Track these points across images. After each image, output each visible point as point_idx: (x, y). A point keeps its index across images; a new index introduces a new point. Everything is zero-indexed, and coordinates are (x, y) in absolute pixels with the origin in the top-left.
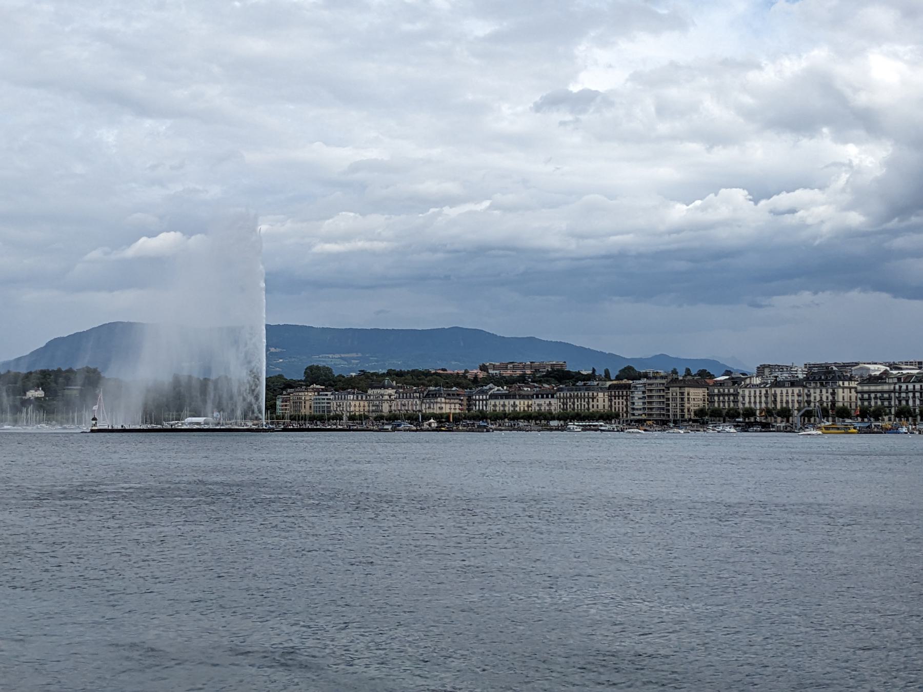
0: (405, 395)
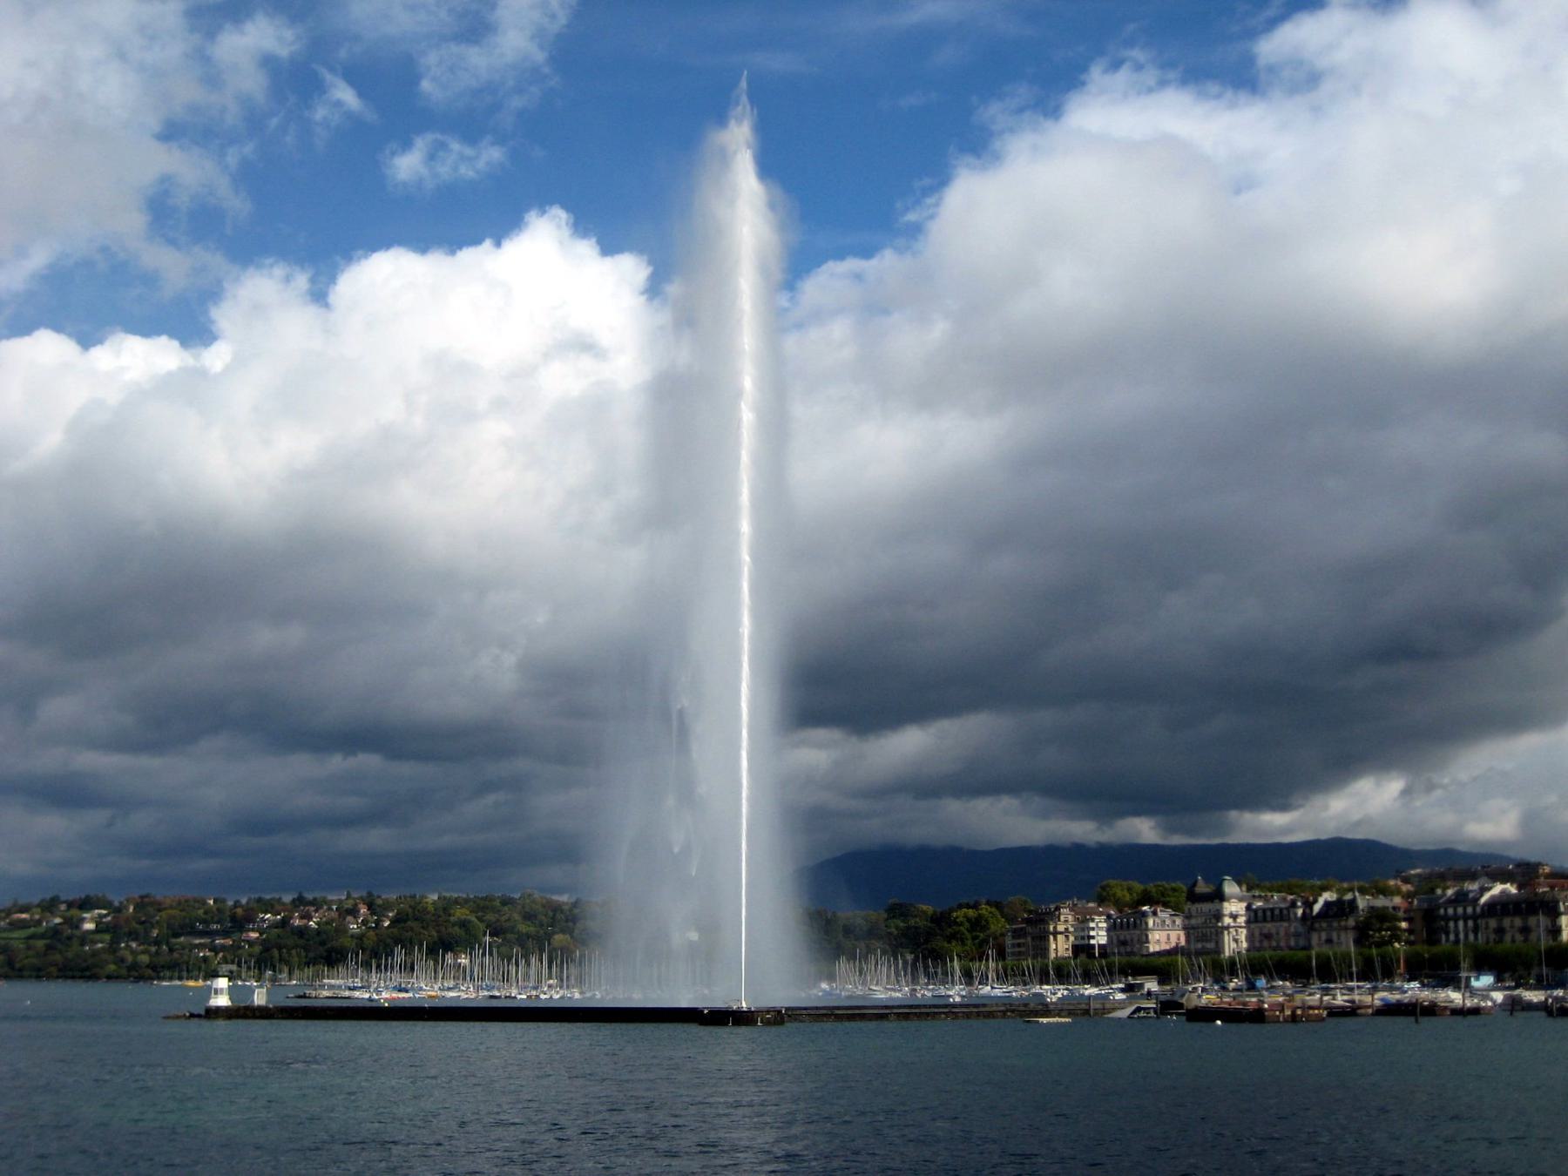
0: (1269, 913)
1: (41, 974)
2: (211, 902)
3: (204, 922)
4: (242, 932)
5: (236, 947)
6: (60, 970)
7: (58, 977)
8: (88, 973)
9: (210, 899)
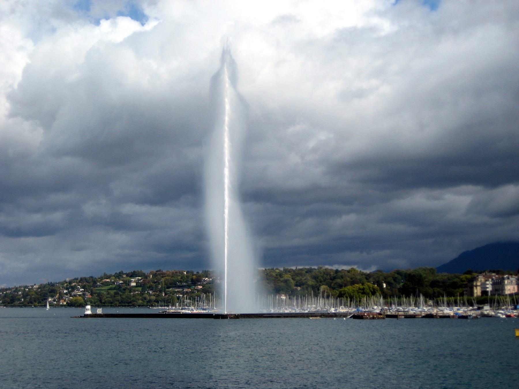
1: (113, 304)
2: (185, 273)
3: (180, 282)
4: (195, 286)
5: (192, 292)
6: (120, 303)
7: (119, 306)
8: (131, 304)
9: (185, 272)
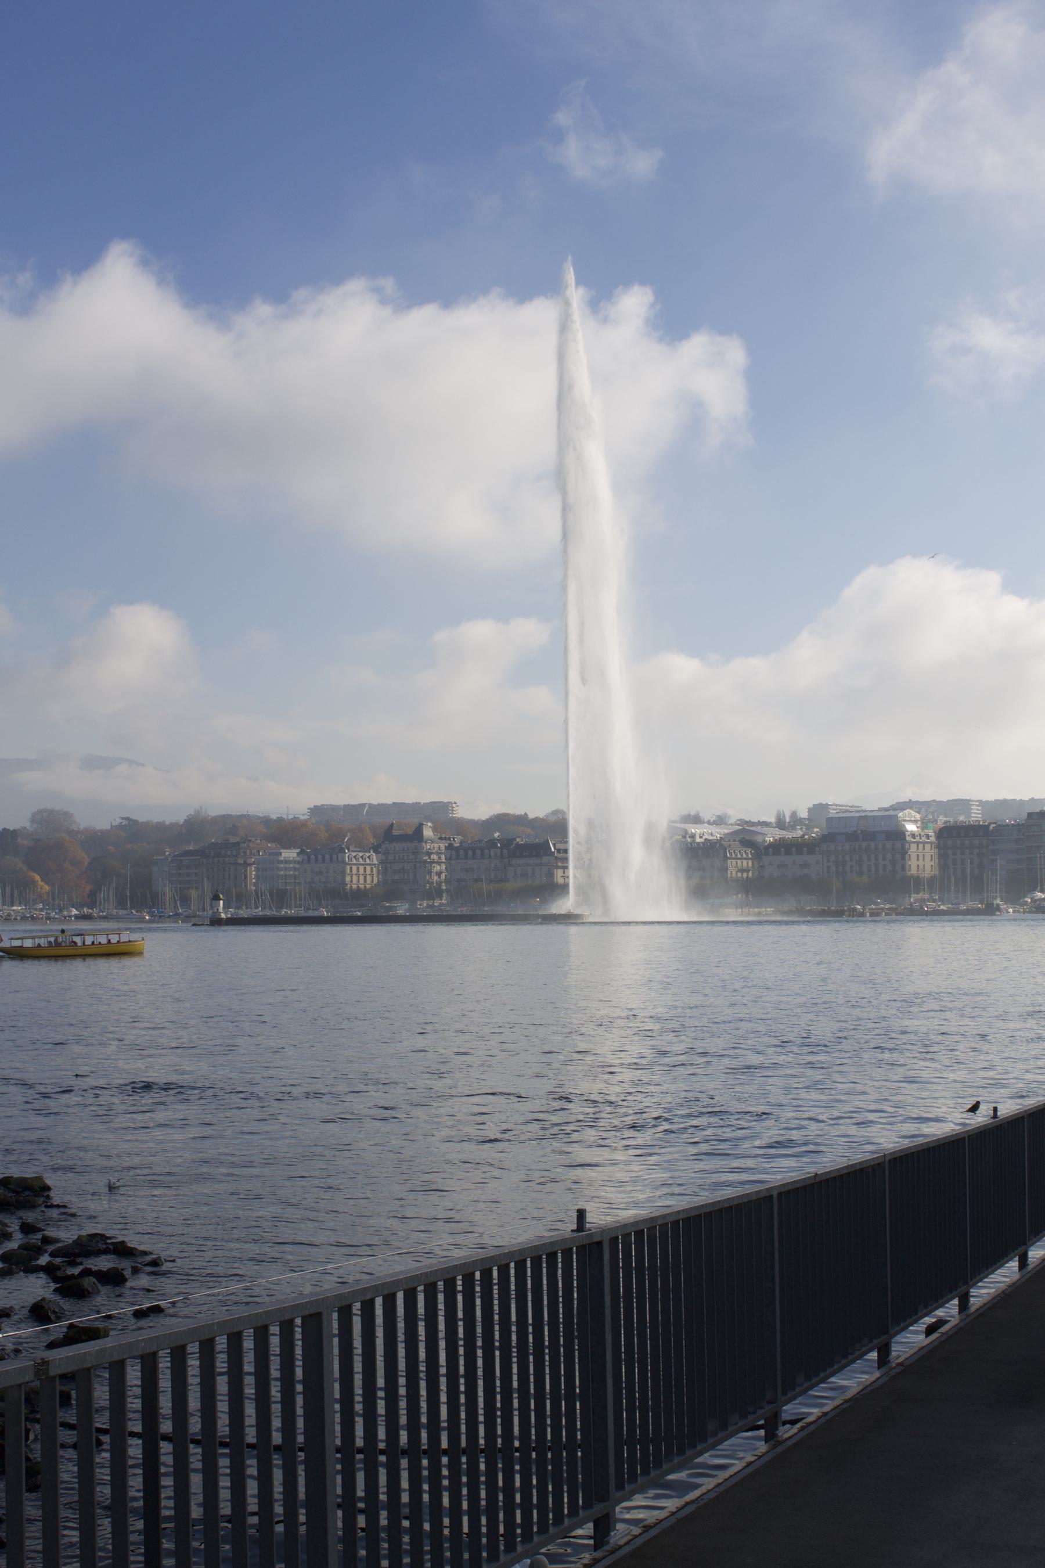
0: (470, 853)
